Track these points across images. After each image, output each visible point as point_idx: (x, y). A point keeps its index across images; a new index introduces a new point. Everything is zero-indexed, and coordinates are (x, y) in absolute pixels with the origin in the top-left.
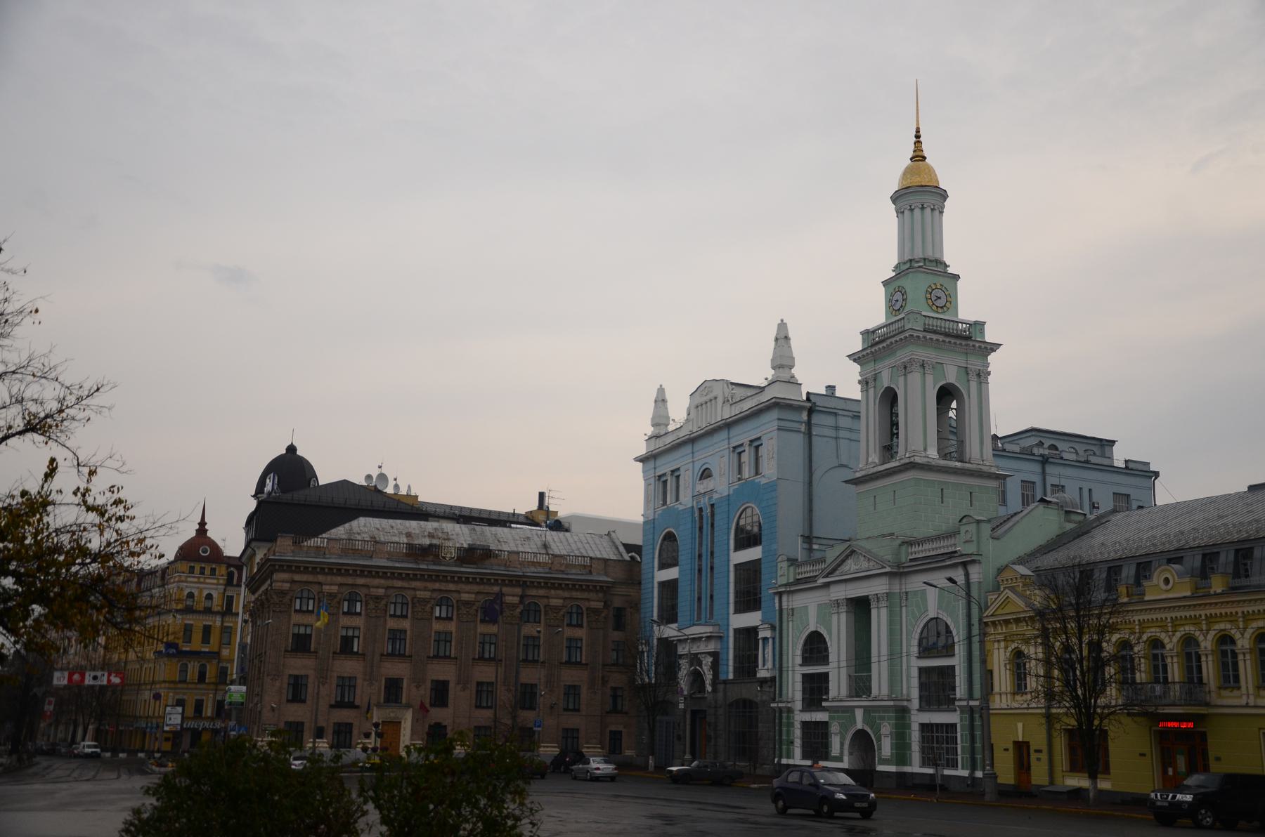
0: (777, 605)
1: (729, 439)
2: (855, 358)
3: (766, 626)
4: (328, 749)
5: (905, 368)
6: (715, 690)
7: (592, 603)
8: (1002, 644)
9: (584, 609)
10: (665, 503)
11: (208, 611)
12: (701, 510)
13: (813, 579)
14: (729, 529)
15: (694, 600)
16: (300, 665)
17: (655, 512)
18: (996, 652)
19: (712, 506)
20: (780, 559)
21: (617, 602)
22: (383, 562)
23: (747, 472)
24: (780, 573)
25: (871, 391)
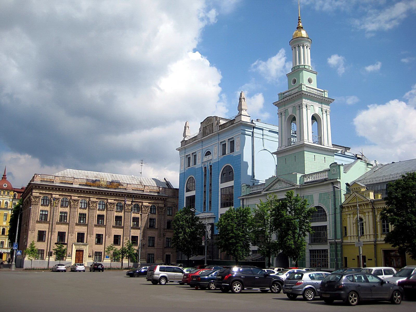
0: (241, 204)
1: (219, 139)
2: (277, 104)
4: (54, 260)
5: (299, 107)
7: (159, 205)
8: (352, 216)
9: (156, 207)
10: (189, 166)
11: (6, 209)
12: (205, 168)
13: (260, 192)
14: (219, 174)
15: (202, 203)
16: (44, 227)
17: (185, 170)
18: (348, 219)
19: (211, 166)
20: (242, 185)
21: (169, 205)
22: (77, 186)
23: (228, 151)
24: (243, 191)
25: (283, 117)
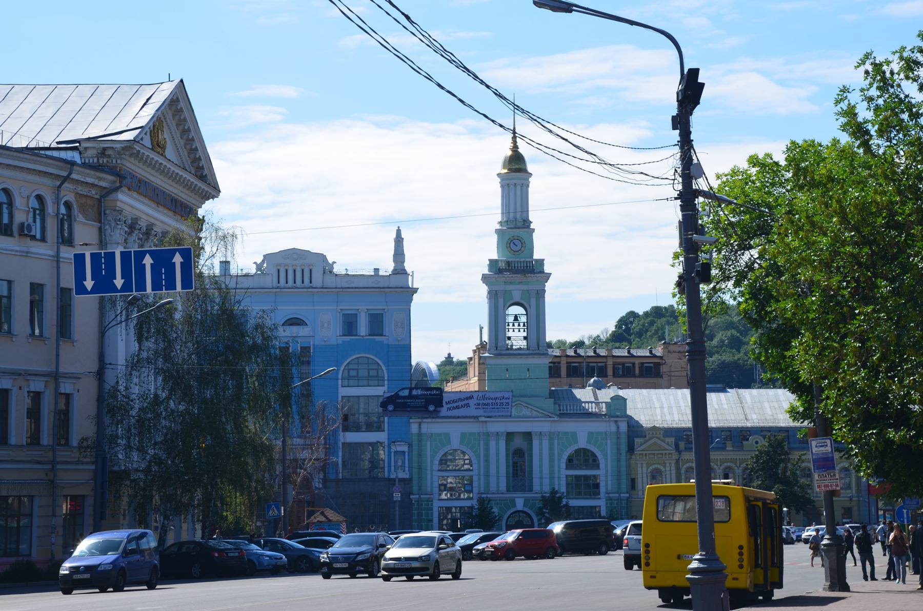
3: (403, 443)
6: (325, 487)
18: (639, 470)
